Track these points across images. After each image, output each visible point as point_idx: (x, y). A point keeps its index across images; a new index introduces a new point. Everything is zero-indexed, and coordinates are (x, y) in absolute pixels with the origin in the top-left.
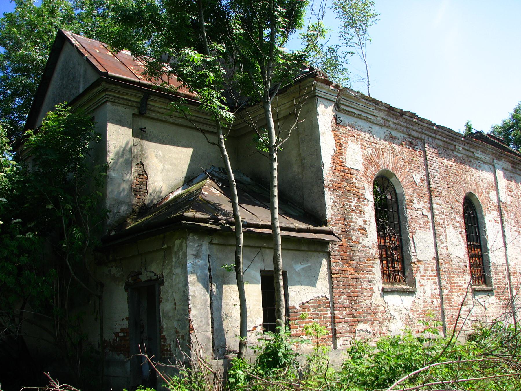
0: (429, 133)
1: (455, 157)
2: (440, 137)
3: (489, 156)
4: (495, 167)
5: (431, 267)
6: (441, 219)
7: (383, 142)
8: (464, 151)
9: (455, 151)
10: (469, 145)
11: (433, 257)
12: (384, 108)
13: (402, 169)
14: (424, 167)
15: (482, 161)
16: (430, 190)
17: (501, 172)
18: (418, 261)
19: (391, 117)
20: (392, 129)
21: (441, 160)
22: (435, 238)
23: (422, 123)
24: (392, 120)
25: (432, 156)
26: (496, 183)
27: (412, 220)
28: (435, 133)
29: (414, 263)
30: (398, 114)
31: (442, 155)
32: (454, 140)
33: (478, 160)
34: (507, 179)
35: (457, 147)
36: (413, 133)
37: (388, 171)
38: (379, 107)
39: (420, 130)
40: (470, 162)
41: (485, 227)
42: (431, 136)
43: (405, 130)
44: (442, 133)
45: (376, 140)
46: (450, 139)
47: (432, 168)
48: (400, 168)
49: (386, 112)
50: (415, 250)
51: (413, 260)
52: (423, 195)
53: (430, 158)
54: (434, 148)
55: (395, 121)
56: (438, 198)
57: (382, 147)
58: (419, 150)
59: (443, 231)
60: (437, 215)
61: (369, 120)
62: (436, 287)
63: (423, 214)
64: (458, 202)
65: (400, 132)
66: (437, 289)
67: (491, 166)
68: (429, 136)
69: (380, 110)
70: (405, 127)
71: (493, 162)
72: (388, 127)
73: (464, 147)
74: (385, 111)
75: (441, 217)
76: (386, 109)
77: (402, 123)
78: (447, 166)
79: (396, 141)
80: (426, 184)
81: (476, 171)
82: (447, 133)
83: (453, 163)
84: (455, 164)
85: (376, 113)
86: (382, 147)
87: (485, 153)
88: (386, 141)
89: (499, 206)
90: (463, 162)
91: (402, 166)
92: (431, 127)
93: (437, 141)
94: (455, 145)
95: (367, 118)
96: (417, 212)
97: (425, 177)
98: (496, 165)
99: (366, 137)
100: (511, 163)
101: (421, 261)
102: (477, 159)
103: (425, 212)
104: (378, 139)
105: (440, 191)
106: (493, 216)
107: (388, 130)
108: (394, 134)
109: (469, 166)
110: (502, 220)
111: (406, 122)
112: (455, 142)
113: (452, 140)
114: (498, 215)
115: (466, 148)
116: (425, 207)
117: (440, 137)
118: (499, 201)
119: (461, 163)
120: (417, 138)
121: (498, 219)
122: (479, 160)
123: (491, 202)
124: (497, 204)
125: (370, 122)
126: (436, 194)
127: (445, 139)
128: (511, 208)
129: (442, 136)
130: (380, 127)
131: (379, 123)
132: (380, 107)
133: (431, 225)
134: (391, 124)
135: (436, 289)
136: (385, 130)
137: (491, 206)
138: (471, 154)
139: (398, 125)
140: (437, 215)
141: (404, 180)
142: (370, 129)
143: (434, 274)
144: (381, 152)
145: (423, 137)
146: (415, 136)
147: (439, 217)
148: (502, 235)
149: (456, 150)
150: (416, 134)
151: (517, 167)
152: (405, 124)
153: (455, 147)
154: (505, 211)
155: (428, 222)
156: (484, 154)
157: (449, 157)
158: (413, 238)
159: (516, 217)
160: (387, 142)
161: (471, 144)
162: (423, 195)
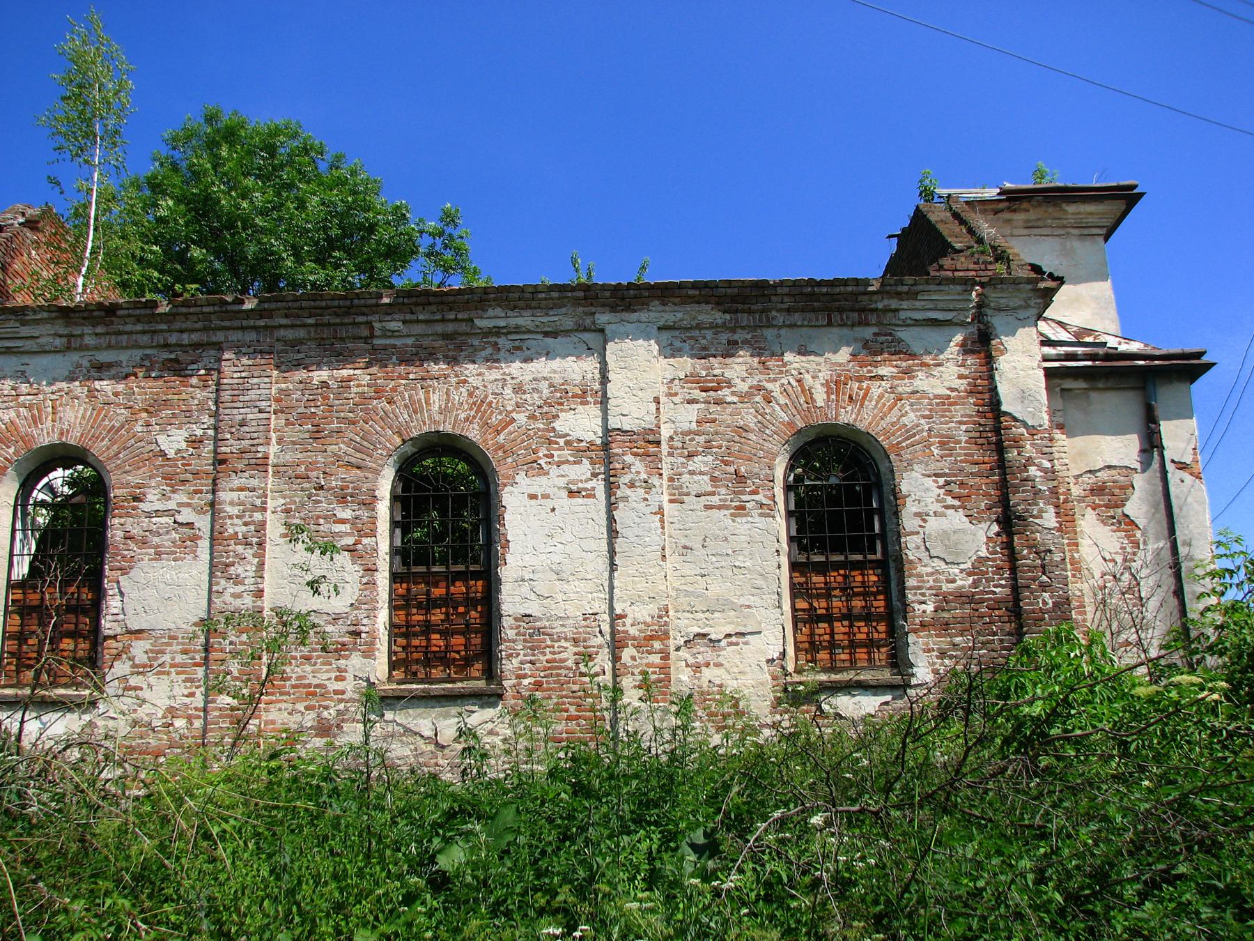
0: (237, 323)
1: (374, 350)
2: (284, 321)
3: (564, 310)
4: (605, 335)
5: (184, 644)
6: (246, 524)
7: (64, 385)
8: (418, 329)
9: (372, 336)
10: (434, 308)
11: (196, 619)
12: (45, 315)
13: (119, 430)
14: (214, 408)
15: (530, 332)
16: (220, 461)
17: (641, 342)
18: (130, 632)
19: (83, 325)
20: (97, 348)
21: (301, 374)
22: (212, 575)
23: (192, 310)
24: (88, 330)
25: (243, 374)
26: (604, 380)
27: (129, 541)
28: (261, 317)
29: (114, 637)
30: (96, 313)
31: (308, 361)
32: (352, 311)
33: (506, 334)
34: (692, 356)
35: (377, 325)
36: (173, 339)
37: (64, 445)
38: (27, 318)
39: (199, 325)
40: (459, 348)
41: (500, 518)
42: (255, 328)
43: (145, 339)
44: (289, 308)
45: (35, 386)
46: (337, 315)
47: (241, 405)
48: (109, 431)
49: (61, 321)
50: (123, 609)
51: (107, 632)
52: (190, 477)
53: (241, 381)
54: (261, 352)
55: (99, 329)
56: (247, 475)
57: (53, 397)
58: (202, 372)
59: (249, 553)
60: (231, 517)
61: (16, 350)
62: (194, 689)
63: (175, 522)
64: (358, 468)
65: (127, 348)
66: (198, 694)
67: (587, 336)
68: (242, 328)
69: (37, 322)
70: (144, 332)
71: (594, 323)
72: (81, 348)
73: (408, 317)
74: (56, 318)
75: (247, 519)
76: (54, 315)
77: (129, 328)
78: (324, 385)
79: (113, 371)
80: (209, 447)
81: (490, 368)
82: (304, 304)
83: (357, 372)
84: (374, 370)
85: (25, 331)
86: (53, 397)
87: (529, 307)
88: (73, 380)
89: (606, 446)
90: (419, 356)
91: (117, 425)
92: (236, 308)
93: (282, 332)
94: (369, 324)
95: (7, 348)
96: (154, 520)
97: (211, 432)
98: (608, 329)
99: (6, 387)
100: (718, 304)
101: (140, 631)
102: (497, 331)
103: (186, 516)
104: (44, 383)
105: (260, 455)
106: (562, 482)
107: (82, 354)
108: (104, 357)
109: (453, 361)
110: (610, 488)
111: (139, 321)
112: (364, 314)
113: (348, 314)
114: (595, 475)
115: (421, 317)
116: (188, 505)
117: (284, 321)
118: (607, 431)
119: (402, 361)
120: (196, 346)
121: (599, 486)
122: (510, 333)
123: (562, 441)
124: (599, 441)
125: (22, 353)
126: (240, 466)
127: (311, 321)
128: (702, 439)
129: (298, 316)
130: (61, 354)
131: (47, 348)
132: (33, 317)
133: (204, 545)
134: (88, 340)
135: (192, 695)
136: (75, 357)
137: (556, 453)
138: (464, 327)
139: (120, 333)
140: (231, 517)
141: (121, 455)
142: (22, 368)
143: (193, 658)
144: (50, 409)
145: (220, 336)
146: (186, 342)
147: (236, 521)
148: (604, 530)
149: (378, 333)
150: (186, 340)
151: (759, 306)
152: (139, 327)
153: (372, 328)
154: (636, 455)
155: (195, 539)
156: (528, 313)
157: (340, 357)
158: (118, 582)
159: (727, 463)
160: (77, 383)
161: (442, 303)
162: (190, 477)
